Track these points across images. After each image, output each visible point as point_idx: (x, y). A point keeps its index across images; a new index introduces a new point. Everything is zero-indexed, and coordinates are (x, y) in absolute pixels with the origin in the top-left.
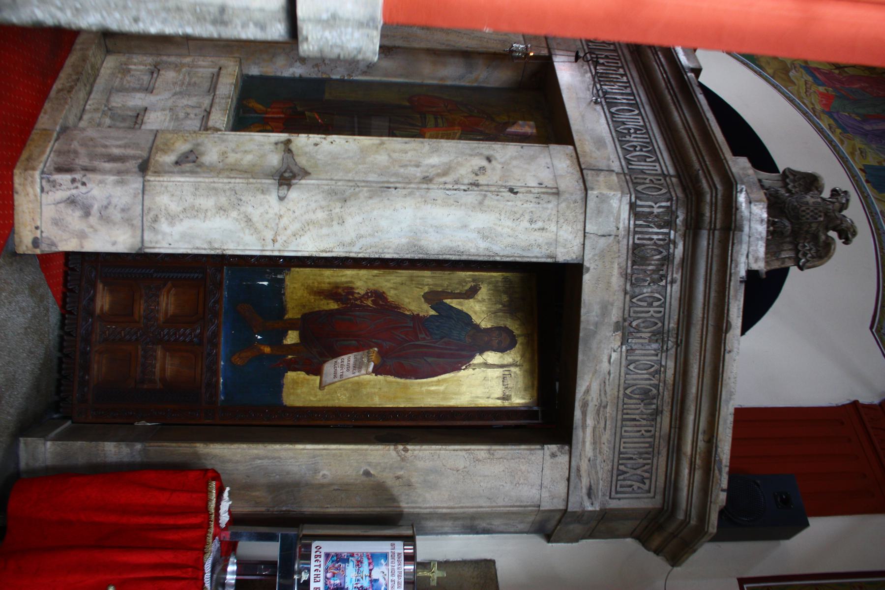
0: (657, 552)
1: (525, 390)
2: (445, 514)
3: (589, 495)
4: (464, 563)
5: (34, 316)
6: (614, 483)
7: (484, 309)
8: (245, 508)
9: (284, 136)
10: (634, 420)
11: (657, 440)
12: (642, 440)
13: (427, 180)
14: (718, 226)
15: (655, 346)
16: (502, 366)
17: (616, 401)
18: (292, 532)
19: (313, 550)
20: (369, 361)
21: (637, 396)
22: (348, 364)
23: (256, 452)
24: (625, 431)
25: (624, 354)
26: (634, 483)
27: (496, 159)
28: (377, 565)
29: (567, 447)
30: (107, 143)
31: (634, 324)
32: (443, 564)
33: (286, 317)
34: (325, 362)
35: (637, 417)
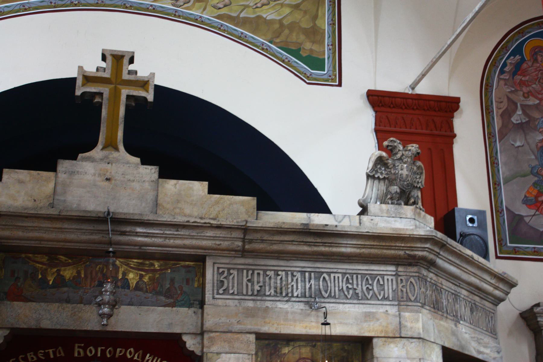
14: (438, 251)
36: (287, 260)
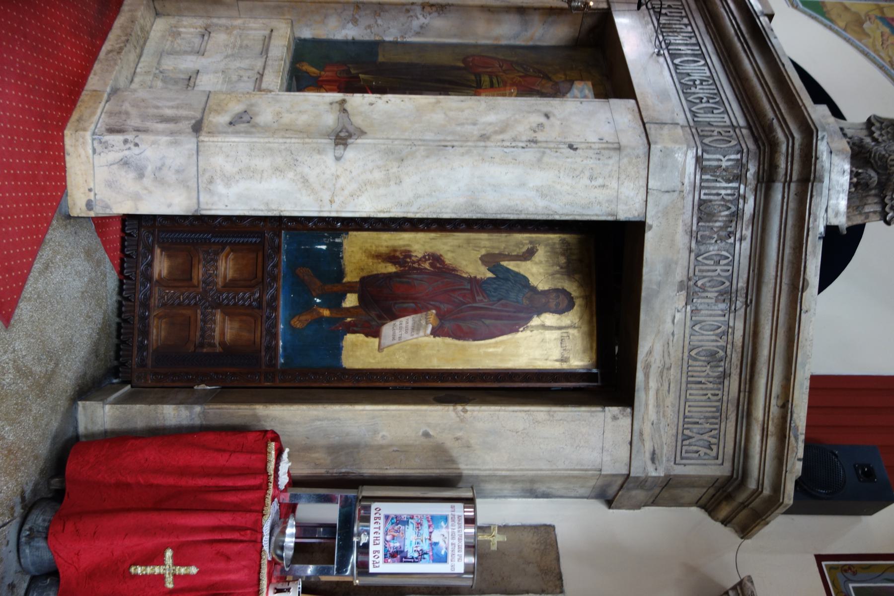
0: (725, 522)
1: (584, 352)
2: (505, 477)
3: (653, 460)
4: (524, 527)
5: (91, 281)
6: (679, 448)
7: (542, 271)
8: (304, 470)
9: (338, 96)
10: (700, 383)
11: (725, 404)
12: (709, 404)
13: (484, 137)
14: (795, 178)
15: (723, 306)
16: (560, 328)
17: (680, 363)
18: (351, 493)
19: (373, 511)
20: (427, 323)
21: (703, 358)
22: (407, 327)
23: (315, 413)
24: (690, 395)
25: (689, 314)
26: (700, 449)
27: (554, 115)
28: (437, 527)
29: (629, 410)
30: (160, 104)
31: (699, 283)
32: (503, 529)
33: (345, 280)
34: (383, 324)
35: (703, 380)
36: (708, 32)
